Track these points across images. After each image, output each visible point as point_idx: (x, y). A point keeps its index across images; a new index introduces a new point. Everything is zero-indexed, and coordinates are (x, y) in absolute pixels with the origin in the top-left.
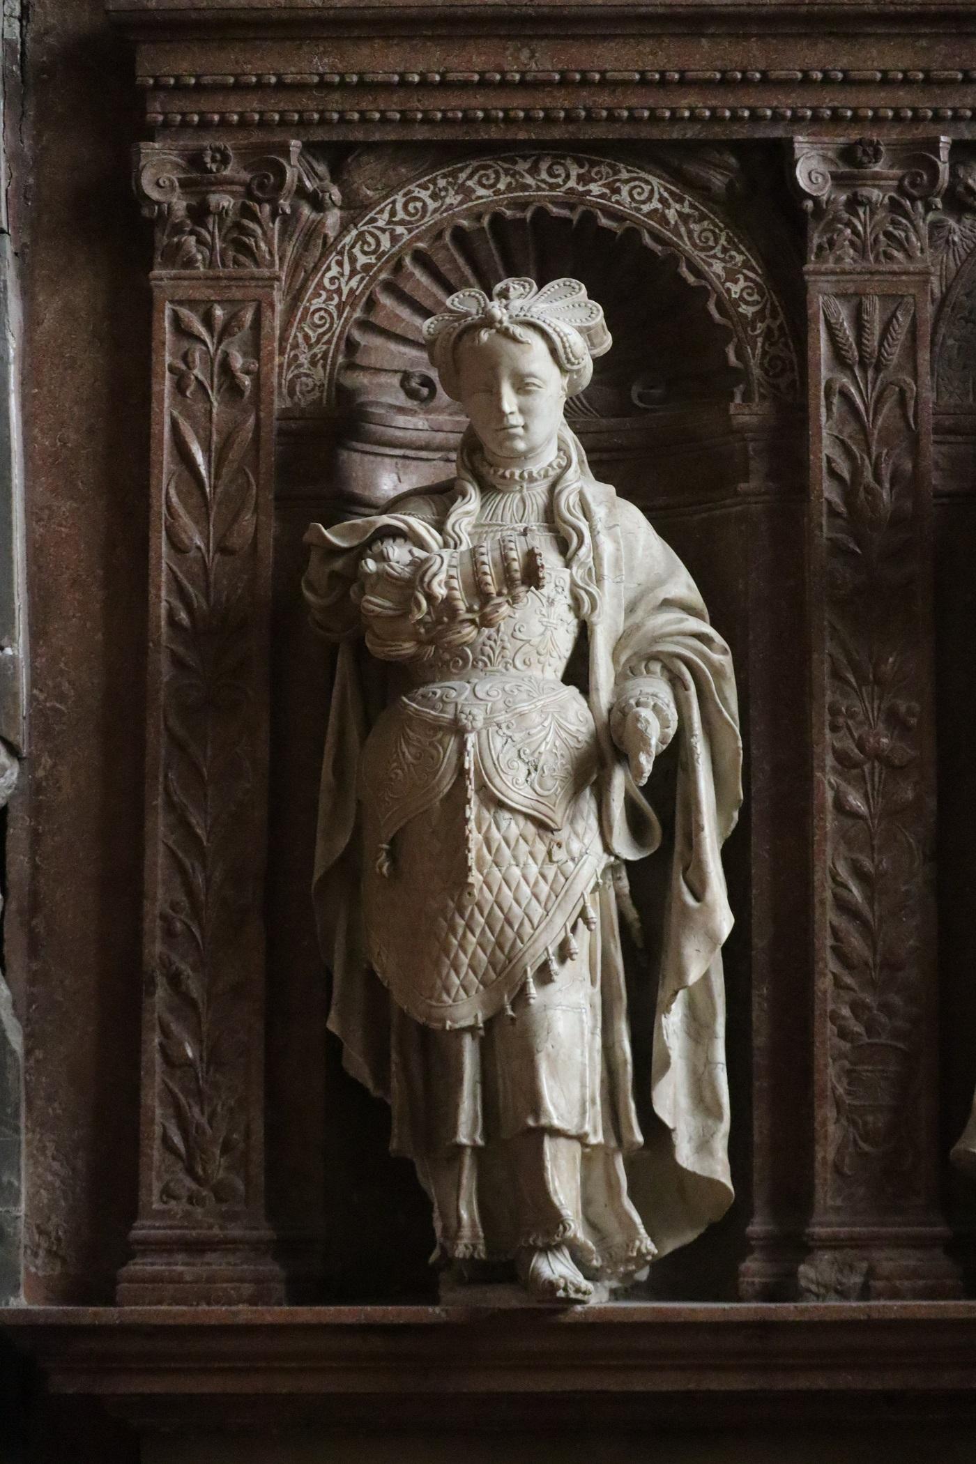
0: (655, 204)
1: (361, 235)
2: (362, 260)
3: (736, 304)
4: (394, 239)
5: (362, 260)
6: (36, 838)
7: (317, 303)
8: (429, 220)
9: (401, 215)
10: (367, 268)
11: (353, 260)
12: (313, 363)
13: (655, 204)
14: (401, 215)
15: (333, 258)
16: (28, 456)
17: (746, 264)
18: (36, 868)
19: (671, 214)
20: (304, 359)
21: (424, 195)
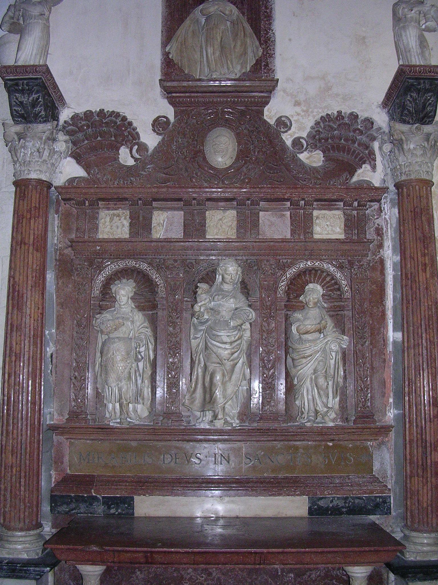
0: (146, 268)
1: (104, 272)
2: (104, 275)
3: (157, 282)
4: (109, 272)
5: (104, 275)
6: (57, 357)
7: (97, 282)
8: (114, 270)
9: (110, 269)
10: (105, 276)
11: (103, 275)
12: (97, 290)
13: (146, 268)
14: (110, 269)
15: (100, 275)
16: (57, 303)
17: (158, 277)
18: (56, 362)
19: (148, 269)
20: (96, 290)
21: (113, 266)
